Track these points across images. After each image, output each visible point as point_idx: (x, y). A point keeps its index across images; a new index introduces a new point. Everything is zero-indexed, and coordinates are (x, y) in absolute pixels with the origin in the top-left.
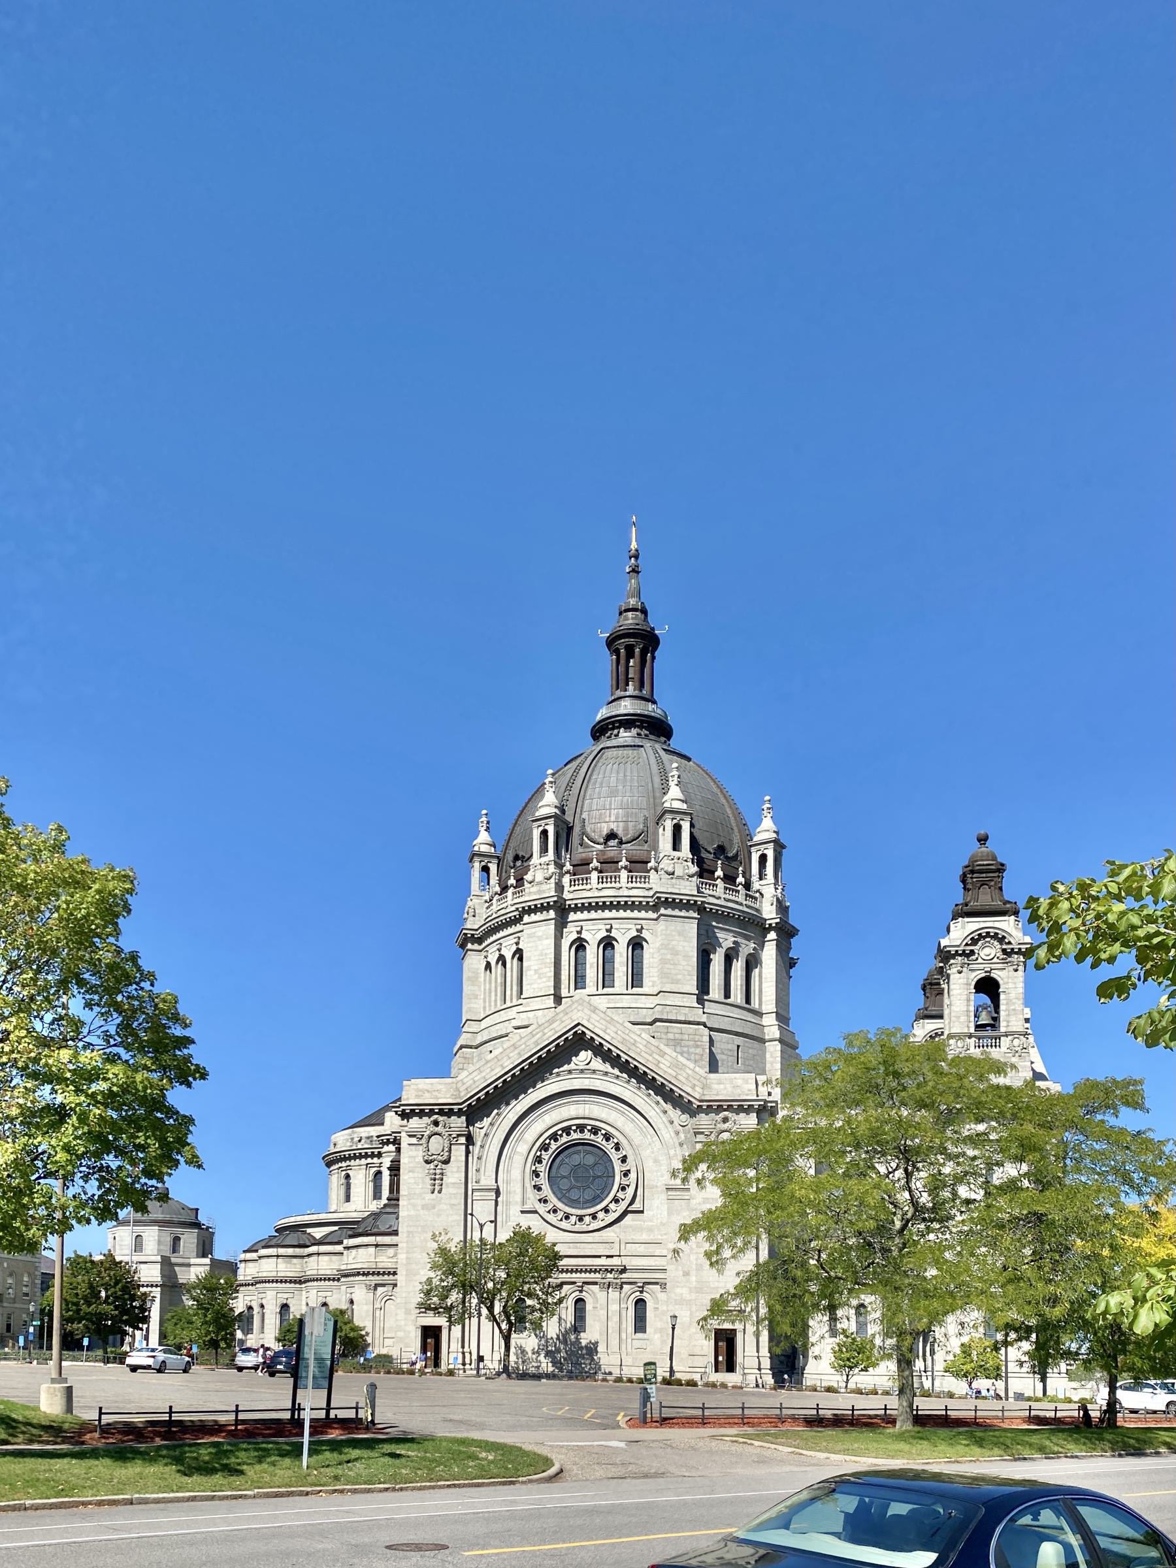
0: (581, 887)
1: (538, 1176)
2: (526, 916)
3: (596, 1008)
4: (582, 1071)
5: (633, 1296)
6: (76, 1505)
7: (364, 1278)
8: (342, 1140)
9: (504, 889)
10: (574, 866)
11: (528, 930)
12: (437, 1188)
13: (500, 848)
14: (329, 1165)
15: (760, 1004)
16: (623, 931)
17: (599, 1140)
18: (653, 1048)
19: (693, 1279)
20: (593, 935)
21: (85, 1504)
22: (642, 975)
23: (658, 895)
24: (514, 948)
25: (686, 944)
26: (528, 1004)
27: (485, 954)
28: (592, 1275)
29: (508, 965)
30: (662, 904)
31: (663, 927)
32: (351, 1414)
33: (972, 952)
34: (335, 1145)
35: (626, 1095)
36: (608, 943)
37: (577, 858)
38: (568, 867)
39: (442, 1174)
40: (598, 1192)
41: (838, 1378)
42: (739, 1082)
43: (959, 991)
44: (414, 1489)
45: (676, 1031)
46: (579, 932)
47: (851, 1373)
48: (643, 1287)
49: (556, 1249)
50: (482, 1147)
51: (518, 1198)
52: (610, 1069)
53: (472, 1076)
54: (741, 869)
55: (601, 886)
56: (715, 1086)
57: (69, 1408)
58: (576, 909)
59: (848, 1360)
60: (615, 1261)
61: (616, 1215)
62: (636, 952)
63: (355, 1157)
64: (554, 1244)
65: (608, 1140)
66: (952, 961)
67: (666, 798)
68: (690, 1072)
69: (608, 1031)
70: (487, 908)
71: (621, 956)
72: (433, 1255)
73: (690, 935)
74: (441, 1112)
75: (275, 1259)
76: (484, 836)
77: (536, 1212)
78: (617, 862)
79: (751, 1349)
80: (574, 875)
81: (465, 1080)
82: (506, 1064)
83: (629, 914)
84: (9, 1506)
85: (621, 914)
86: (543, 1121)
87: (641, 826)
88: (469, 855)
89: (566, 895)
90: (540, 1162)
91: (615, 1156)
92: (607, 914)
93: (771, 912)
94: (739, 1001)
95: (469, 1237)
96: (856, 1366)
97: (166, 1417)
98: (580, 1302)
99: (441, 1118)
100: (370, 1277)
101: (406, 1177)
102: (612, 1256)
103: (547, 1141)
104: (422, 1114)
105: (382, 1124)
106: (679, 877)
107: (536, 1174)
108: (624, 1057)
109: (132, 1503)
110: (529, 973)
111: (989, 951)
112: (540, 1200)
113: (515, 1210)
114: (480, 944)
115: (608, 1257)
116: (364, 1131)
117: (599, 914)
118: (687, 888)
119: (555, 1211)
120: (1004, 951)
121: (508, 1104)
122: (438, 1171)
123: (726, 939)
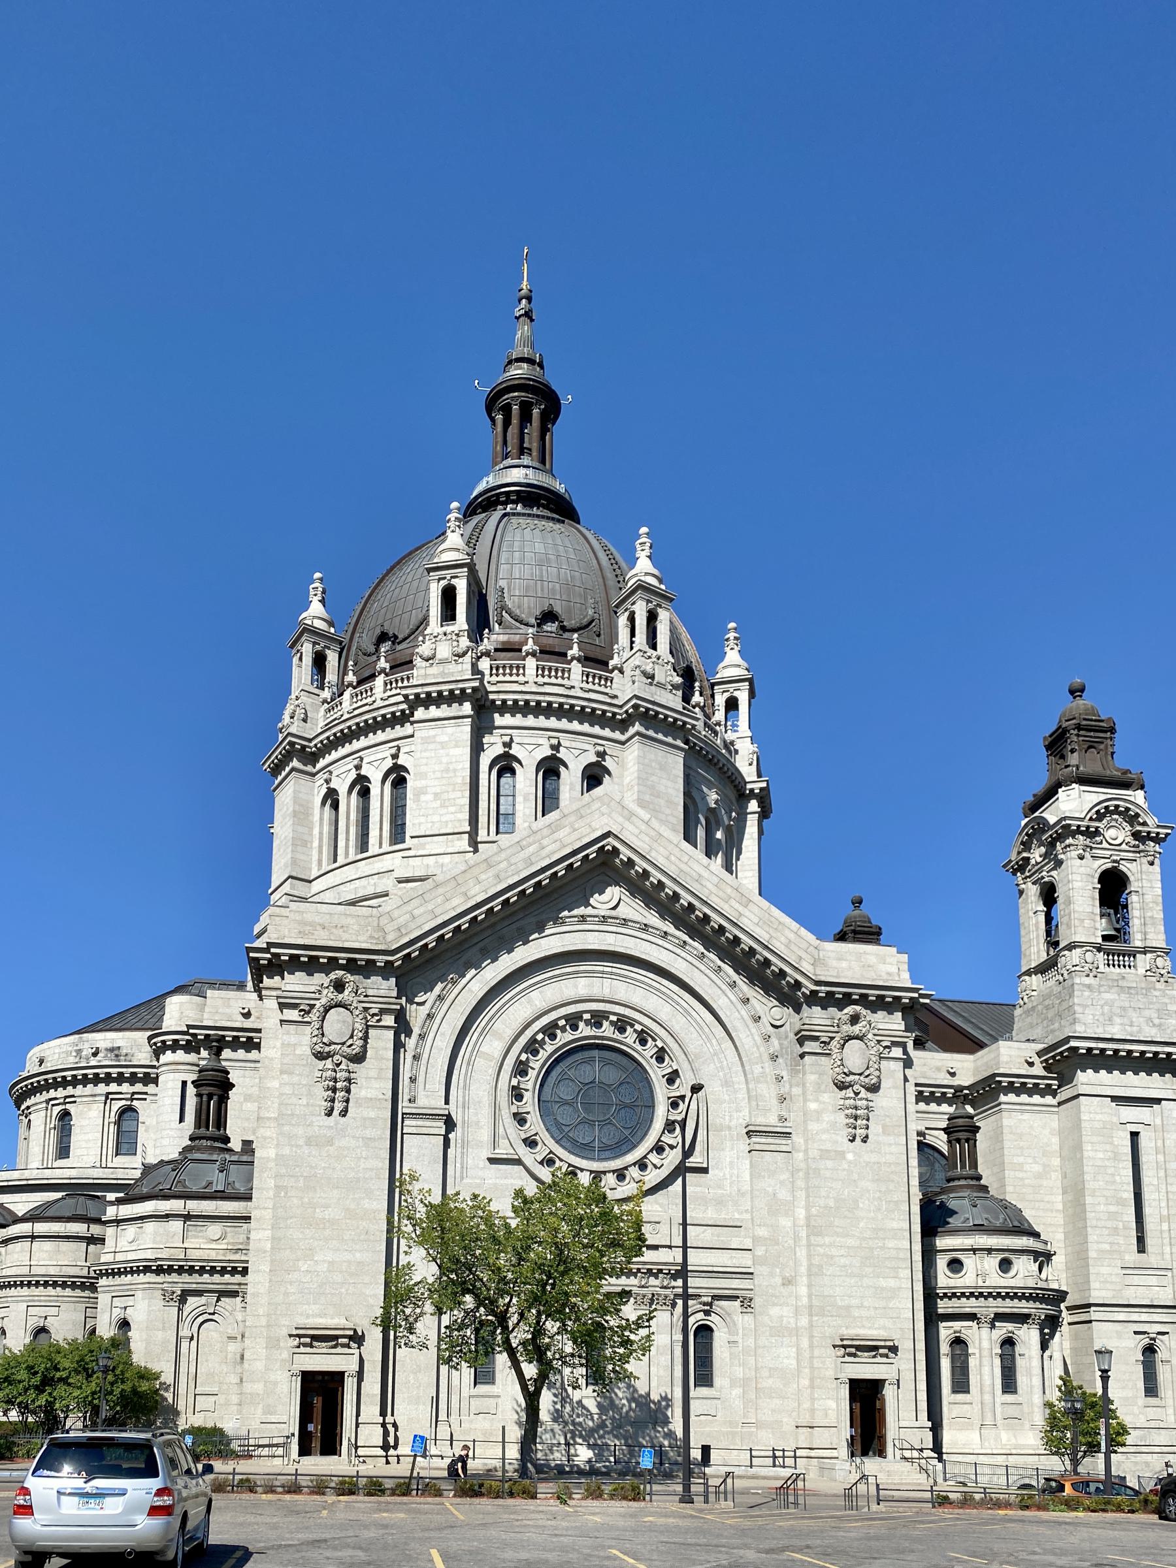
1: (519, 1097)
4: (604, 920)
7: (160, 1279)
11: (422, 731)
12: (338, 1106)
16: (577, 752)
25: (669, 784)
26: (423, 846)
33: (1097, 832)
39: (349, 1080)
43: (1080, 884)
46: (508, 745)
50: (422, 1037)
51: (485, 1135)
55: (540, 680)
56: (834, 963)
58: (504, 708)
66: (1070, 841)
73: (674, 772)
74: (352, 966)
81: (396, 914)
82: (472, 892)
83: (586, 728)
85: (575, 726)
86: (530, 1001)
87: (591, 612)
92: (553, 722)
99: (349, 977)
100: (174, 1277)
103: (540, 1037)
111: (1117, 833)
112: (525, 1141)
120: (1136, 835)
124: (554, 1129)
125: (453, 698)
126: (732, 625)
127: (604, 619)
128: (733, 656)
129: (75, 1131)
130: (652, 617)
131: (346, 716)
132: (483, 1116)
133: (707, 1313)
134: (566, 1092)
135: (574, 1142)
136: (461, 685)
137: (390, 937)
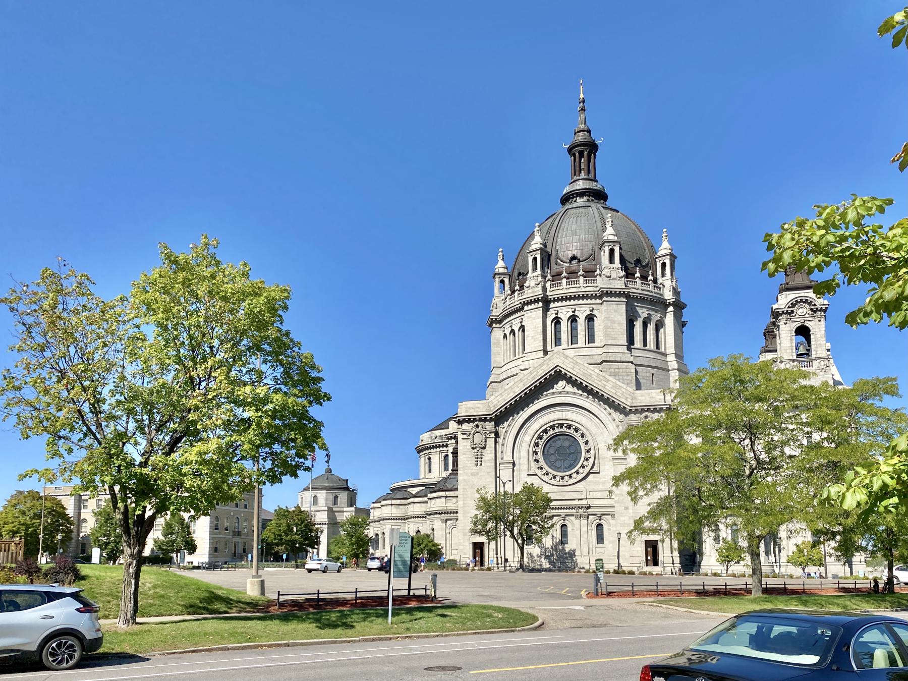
0: (557, 288)
1: (536, 454)
2: (526, 307)
3: (567, 356)
5: (595, 522)
6: (256, 647)
8: (426, 438)
9: (513, 292)
10: (552, 276)
12: (479, 463)
13: (510, 269)
14: (419, 452)
15: (665, 349)
16: (582, 311)
17: (572, 432)
18: (601, 377)
19: (631, 511)
20: (565, 315)
21: (262, 646)
22: (594, 336)
23: (602, 290)
24: (519, 325)
26: (529, 356)
27: (503, 329)
28: (571, 510)
29: (516, 335)
30: (605, 294)
31: (605, 308)
32: (422, 592)
34: (422, 441)
35: (586, 405)
36: (573, 319)
37: (554, 272)
38: (549, 277)
39: (482, 455)
40: (572, 462)
41: (722, 568)
42: (654, 395)
44: (454, 635)
45: (615, 367)
47: (729, 564)
48: (601, 517)
49: (549, 496)
50: (504, 438)
51: (526, 467)
53: (497, 398)
54: (650, 271)
55: (568, 286)
56: (640, 398)
57: (263, 592)
58: (554, 301)
59: (727, 557)
60: (584, 502)
61: (584, 475)
62: (590, 323)
63: (433, 447)
64: (547, 493)
65: (577, 431)
67: (605, 234)
68: (624, 390)
69: (575, 369)
70: (504, 303)
71: (581, 326)
72: (477, 501)
74: (480, 420)
75: (390, 507)
76: (501, 263)
77: (536, 475)
78: (578, 273)
79: (667, 552)
80: (553, 281)
81: (493, 401)
83: (585, 301)
84: (219, 648)
85: (581, 302)
87: (591, 251)
88: (492, 275)
89: (548, 293)
90: (538, 446)
91: (581, 441)
92: (572, 302)
93: (669, 295)
94: (652, 348)
95: (498, 490)
96: (732, 560)
97: (316, 596)
98: (563, 526)
99: (480, 423)
101: (462, 457)
102: (581, 499)
103: (541, 434)
104: (469, 421)
105: (448, 428)
106: (613, 279)
107: (536, 453)
108: (584, 384)
109: (289, 646)
110: (528, 338)
112: (538, 468)
113: (524, 475)
114: (500, 324)
115: (579, 499)
116: (438, 433)
117: (568, 303)
118: (619, 285)
119: (547, 474)
121: (518, 413)
122: (479, 454)
123: (643, 312)
124: (548, 463)
125: (536, 301)
126: (665, 230)
129: (432, 464)
131: (508, 307)
132: (524, 461)
134: (551, 451)
136: (538, 297)
137: (492, 409)
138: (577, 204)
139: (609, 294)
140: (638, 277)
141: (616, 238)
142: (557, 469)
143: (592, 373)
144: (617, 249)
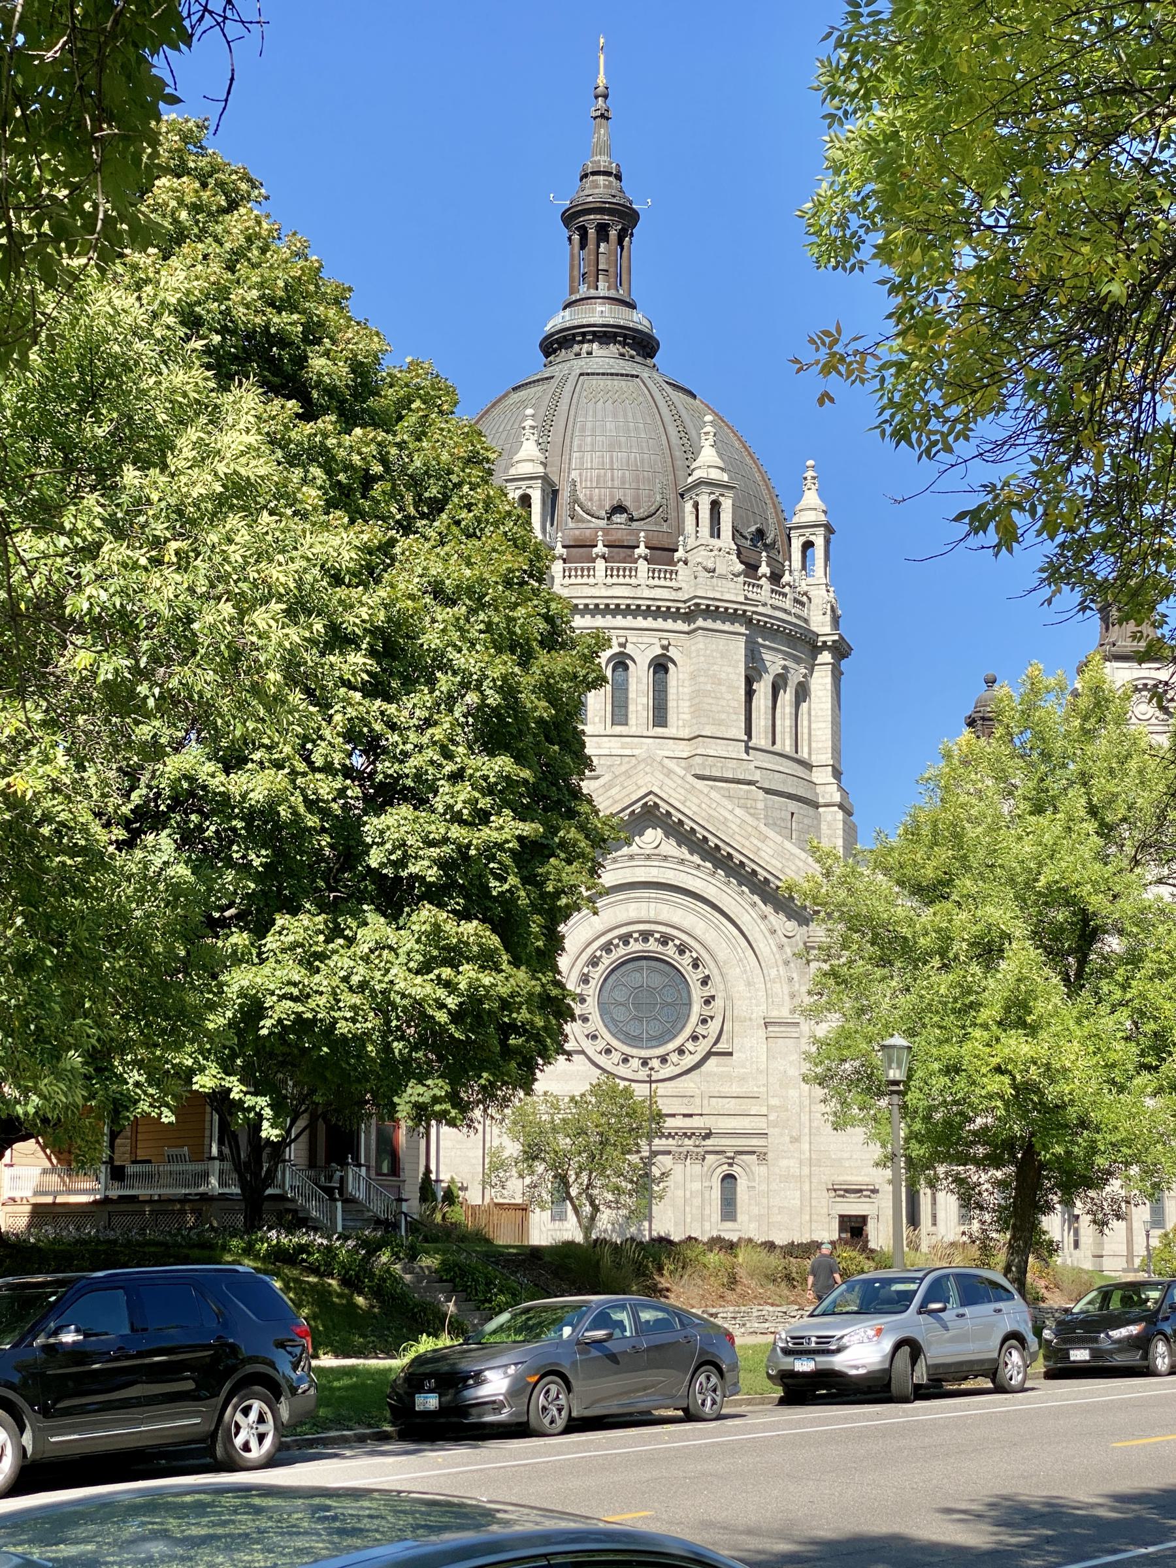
0: (579, 580)
4: (648, 857)
17: (670, 953)
35: (710, 892)
52: (688, 856)
55: (609, 581)
61: (697, 1058)
68: (801, 864)
87: (658, 497)
106: (720, 577)
118: (732, 592)
119: (608, 1051)
127: (672, 503)
128: (811, 498)
130: (715, 505)
133: (730, 1165)
134: (620, 995)
135: (627, 1034)
138: (593, 365)
139: (711, 613)
140: (764, 575)
141: (725, 477)
142: (633, 1040)
143: (730, 817)
144: (727, 505)
